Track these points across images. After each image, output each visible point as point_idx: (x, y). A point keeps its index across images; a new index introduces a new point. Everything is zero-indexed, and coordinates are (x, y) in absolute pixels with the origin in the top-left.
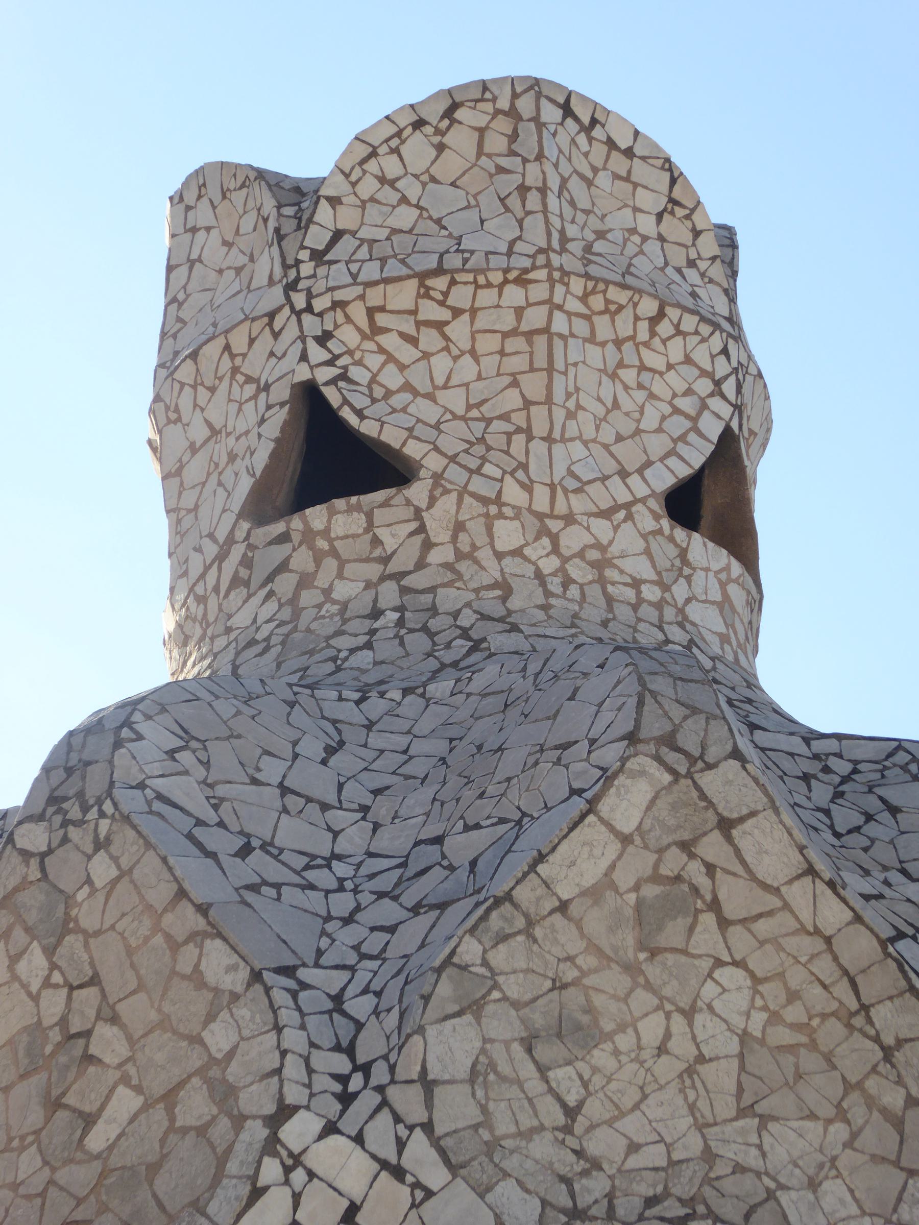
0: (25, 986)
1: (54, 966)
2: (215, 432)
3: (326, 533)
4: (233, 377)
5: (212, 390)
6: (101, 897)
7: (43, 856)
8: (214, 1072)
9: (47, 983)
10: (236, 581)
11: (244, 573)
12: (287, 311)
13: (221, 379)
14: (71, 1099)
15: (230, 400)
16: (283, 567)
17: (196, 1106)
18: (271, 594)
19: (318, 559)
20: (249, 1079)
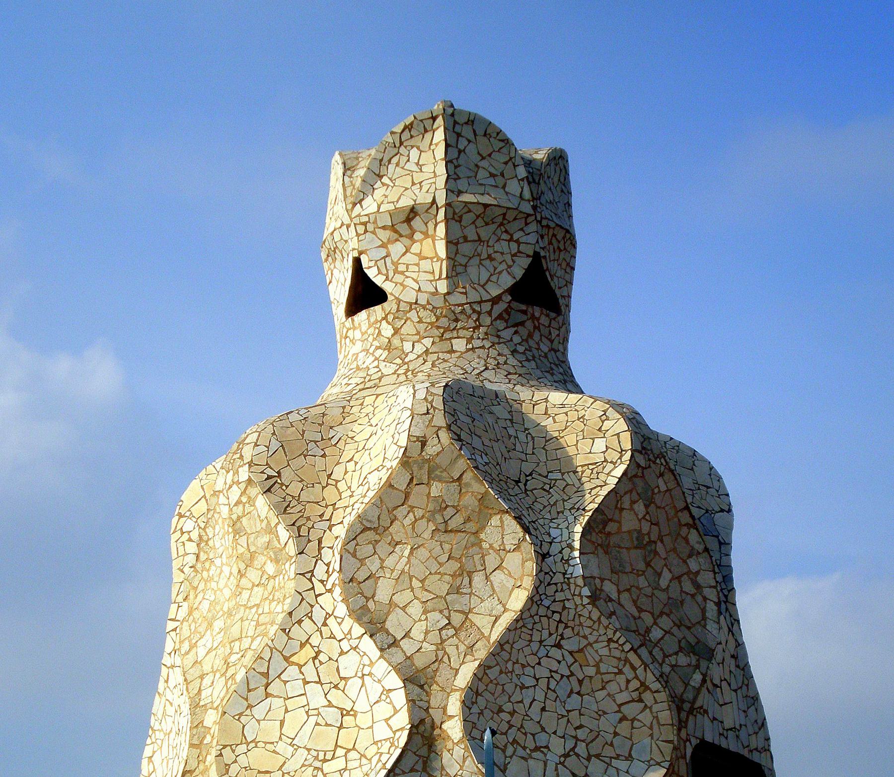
0: (637, 515)
1: (648, 513)
2: (480, 240)
3: (538, 319)
4: (499, 226)
5: (487, 224)
6: (662, 494)
7: (643, 468)
8: (691, 576)
9: (644, 518)
10: (500, 317)
11: (505, 315)
12: (533, 217)
13: (493, 223)
14: (652, 564)
15: (494, 233)
16: (522, 324)
17: (688, 587)
18: (516, 332)
19: (535, 327)
20: (706, 585)
